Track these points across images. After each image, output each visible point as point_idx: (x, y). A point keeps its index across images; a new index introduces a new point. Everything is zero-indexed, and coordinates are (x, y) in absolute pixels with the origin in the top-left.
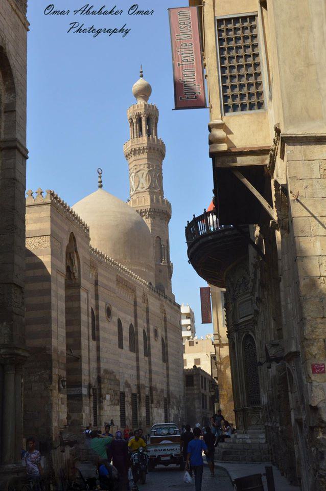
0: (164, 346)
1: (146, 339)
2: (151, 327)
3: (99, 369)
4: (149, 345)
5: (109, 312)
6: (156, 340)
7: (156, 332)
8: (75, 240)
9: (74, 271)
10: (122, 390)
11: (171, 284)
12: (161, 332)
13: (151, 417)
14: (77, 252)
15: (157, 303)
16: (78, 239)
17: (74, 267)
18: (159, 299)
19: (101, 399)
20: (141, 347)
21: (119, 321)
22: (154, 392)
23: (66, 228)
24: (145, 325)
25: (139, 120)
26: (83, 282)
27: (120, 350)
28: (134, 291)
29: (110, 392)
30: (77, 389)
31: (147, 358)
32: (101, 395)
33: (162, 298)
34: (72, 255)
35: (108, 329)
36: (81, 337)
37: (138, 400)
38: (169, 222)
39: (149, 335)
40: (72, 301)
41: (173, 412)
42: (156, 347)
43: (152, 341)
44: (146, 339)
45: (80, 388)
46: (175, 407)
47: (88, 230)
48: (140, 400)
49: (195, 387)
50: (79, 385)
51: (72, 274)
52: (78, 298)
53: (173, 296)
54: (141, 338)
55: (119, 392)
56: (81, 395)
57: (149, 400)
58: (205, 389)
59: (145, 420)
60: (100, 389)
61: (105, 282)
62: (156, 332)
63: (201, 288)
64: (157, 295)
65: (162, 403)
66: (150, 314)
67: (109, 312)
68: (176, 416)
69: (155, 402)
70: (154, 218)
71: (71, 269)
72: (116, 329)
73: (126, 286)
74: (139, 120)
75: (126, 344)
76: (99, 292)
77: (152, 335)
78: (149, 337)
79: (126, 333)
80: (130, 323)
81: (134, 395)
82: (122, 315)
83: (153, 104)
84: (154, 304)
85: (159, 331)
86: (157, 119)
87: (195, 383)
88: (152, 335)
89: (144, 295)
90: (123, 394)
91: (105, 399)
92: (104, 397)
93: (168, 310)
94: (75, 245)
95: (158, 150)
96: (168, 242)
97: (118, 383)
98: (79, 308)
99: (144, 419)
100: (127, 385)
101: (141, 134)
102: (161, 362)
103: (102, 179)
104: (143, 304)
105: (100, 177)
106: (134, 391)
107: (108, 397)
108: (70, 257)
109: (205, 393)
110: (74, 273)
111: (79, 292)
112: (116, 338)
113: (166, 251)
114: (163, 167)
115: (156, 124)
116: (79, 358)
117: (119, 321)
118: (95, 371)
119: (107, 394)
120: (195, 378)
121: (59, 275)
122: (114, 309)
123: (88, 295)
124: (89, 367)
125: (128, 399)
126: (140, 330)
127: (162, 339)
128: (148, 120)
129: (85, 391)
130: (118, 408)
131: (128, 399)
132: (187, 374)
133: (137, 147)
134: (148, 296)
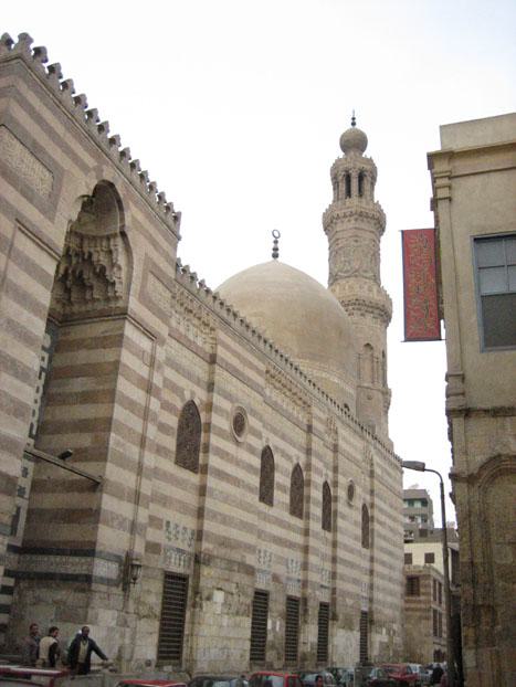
0: (367, 519)
1: (328, 499)
2: (343, 481)
3: (199, 535)
4: (336, 512)
5: (239, 424)
6: (350, 506)
7: (351, 491)
8: (121, 208)
9: (117, 280)
10: (261, 586)
11: (387, 422)
12: (361, 495)
13: (330, 646)
14: (123, 235)
15: (359, 444)
16: (133, 214)
17: (115, 269)
18: (363, 438)
19: (197, 599)
20: (316, 511)
21: (267, 455)
22: (339, 599)
23: (90, 161)
24: (330, 474)
25: (348, 178)
26: (134, 305)
27: (263, 507)
28: (306, 406)
29: (227, 586)
30: (83, 560)
31: (329, 535)
32: (196, 593)
33: (369, 438)
34: (112, 243)
35: (231, 460)
36: (109, 430)
37: (301, 612)
38: (387, 325)
39: (336, 492)
40: (104, 348)
41: (378, 638)
42: (348, 520)
43: (341, 507)
44: (328, 499)
45: (89, 559)
46: (384, 631)
47: (177, 218)
48: (306, 611)
49: (422, 598)
50: (88, 551)
51: (110, 288)
52: (118, 341)
53: (392, 444)
54: (316, 494)
55: (251, 592)
56: (85, 581)
57: (326, 614)
58: (440, 603)
59: (315, 651)
60: (197, 575)
61: (234, 361)
62: (351, 491)
63: (403, 232)
64: (358, 429)
65: (357, 620)
66: (340, 456)
67: (239, 424)
68: (385, 647)
69: (341, 617)
70: (362, 315)
71: (107, 273)
72: (257, 462)
73: (290, 390)
74: (348, 178)
75: (282, 497)
76: (217, 378)
77: (342, 493)
78: (336, 499)
79: (282, 478)
80: (295, 462)
81: (292, 601)
82: (274, 441)
83: (369, 157)
84: (350, 442)
85: (358, 490)
86: (374, 179)
87: (422, 590)
88: (342, 493)
89: (328, 422)
90: (261, 598)
91: (209, 598)
92: (205, 594)
93: (377, 459)
94: (122, 219)
95: (373, 218)
96: (384, 355)
97: (250, 571)
98: (117, 363)
99: (312, 648)
100: (276, 578)
101: (349, 193)
102: (358, 545)
103: (279, 245)
104: (326, 437)
105: (276, 242)
106: (295, 591)
107: (219, 597)
108: (109, 245)
109: (439, 609)
110: (114, 284)
111: (122, 328)
112: (255, 481)
113: (381, 372)
114: (381, 245)
115: (373, 184)
116: (98, 483)
117: (267, 455)
118: (188, 535)
119: (220, 589)
120: (422, 582)
121: (19, 233)
122: (251, 421)
123: (154, 349)
124: (136, 513)
125: (277, 606)
126: (318, 480)
127: (364, 507)
128: (361, 177)
129: (104, 569)
130: (247, 622)
131: (277, 606)
132: (409, 574)
133: (341, 213)
134: (338, 424)
